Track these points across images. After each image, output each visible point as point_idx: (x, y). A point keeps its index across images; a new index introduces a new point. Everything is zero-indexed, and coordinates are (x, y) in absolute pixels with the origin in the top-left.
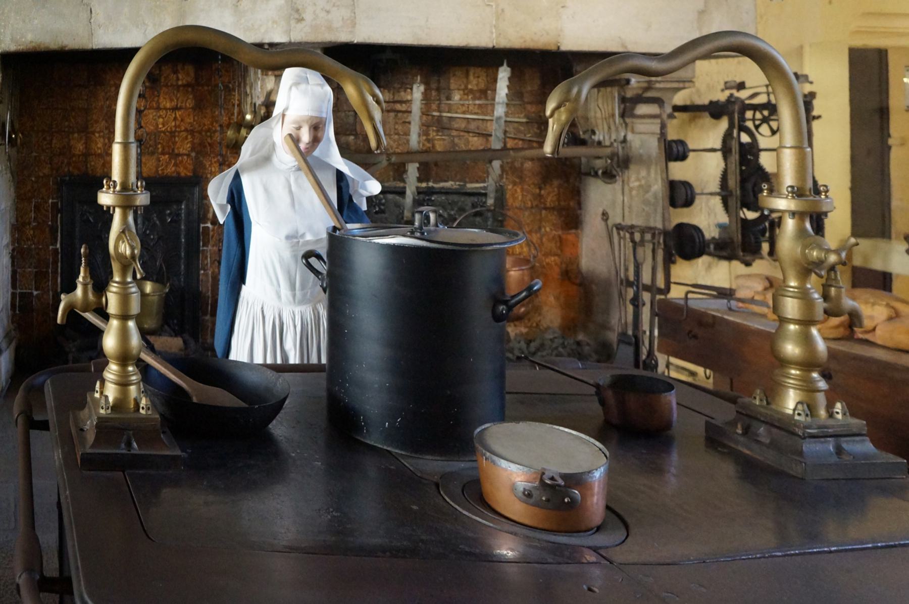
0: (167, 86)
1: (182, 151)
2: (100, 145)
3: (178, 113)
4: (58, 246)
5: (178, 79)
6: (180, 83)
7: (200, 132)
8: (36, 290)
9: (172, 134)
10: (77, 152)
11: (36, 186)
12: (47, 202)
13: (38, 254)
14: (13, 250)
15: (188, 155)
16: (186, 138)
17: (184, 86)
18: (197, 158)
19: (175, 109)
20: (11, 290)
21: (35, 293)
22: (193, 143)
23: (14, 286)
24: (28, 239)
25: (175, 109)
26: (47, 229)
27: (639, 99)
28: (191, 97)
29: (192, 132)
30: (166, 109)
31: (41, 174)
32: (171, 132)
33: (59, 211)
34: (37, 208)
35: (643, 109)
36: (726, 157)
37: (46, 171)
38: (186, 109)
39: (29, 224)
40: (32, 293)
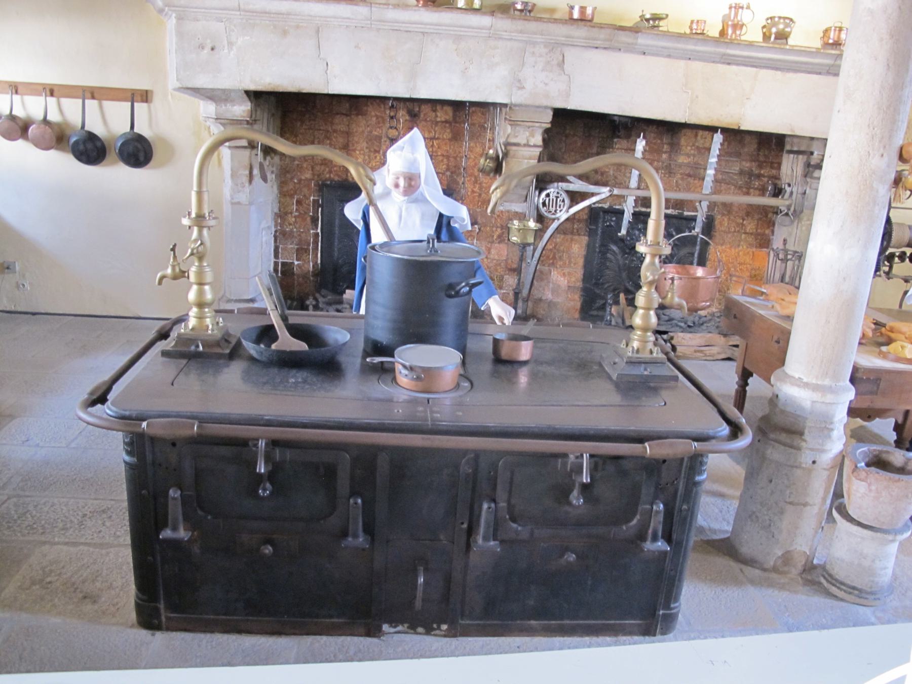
0: (426, 120)
4: (319, 231)
5: (437, 116)
6: (439, 119)
8: (297, 260)
11: (297, 186)
12: (308, 199)
14: (276, 232)
16: (442, 161)
17: (443, 122)
18: (451, 176)
20: (273, 260)
21: (296, 263)
22: (448, 165)
23: (276, 255)
24: (290, 224)
26: (309, 219)
28: (448, 131)
29: (448, 157)
31: (303, 178)
33: (319, 206)
34: (299, 202)
37: (308, 175)
38: (444, 139)
39: (291, 213)
40: (293, 263)
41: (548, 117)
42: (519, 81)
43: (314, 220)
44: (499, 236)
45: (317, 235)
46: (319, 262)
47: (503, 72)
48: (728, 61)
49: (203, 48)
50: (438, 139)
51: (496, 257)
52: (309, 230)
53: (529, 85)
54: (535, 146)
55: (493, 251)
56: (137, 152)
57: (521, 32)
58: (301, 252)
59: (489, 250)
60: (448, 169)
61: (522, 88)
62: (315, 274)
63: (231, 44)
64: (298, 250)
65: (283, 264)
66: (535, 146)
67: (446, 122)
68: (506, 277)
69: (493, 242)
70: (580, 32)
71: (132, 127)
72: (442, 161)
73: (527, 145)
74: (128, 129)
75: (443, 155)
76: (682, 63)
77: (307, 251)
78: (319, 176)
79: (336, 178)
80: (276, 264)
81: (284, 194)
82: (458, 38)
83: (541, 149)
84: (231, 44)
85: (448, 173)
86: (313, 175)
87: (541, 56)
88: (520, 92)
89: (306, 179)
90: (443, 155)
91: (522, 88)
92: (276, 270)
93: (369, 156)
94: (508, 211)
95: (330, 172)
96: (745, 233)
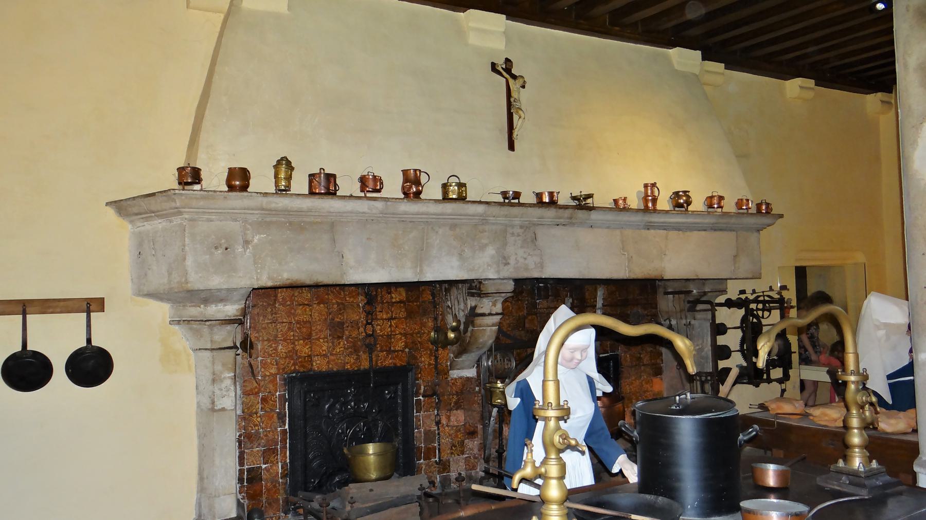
1: (397, 348)
2: (324, 348)
3: (393, 322)
4: (287, 427)
5: (392, 298)
6: (394, 300)
7: (412, 335)
9: (389, 337)
10: (303, 355)
13: (266, 436)
14: (240, 436)
15: (403, 351)
19: (390, 319)
21: (264, 466)
22: (406, 342)
23: (241, 463)
25: (390, 319)
27: (698, 301)
29: (405, 335)
30: (383, 319)
32: (388, 336)
35: (700, 307)
36: (743, 331)
37: (273, 371)
39: (256, 413)
41: (510, 286)
42: (504, 258)
43: (281, 417)
44: (456, 403)
45: (284, 431)
46: (288, 461)
47: (491, 251)
48: (649, 227)
49: (216, 248)
50: (395, 318)
51: (456, 424)
52: (276, 429)
53: (512, 261)
54: (497, 314)
55: (452, 418)
56: (91, 367)
57: (506, 216)
58: (269, 453)
59: (448, 418)
60: (406, 347)
61: (507, 264)
62: (284, 476)
63: (247, 243)
64: (264, 452)
65: (249, 470)
66: (497, 314)
67: (401, 302)
68: (466, 441)
69: (451, 410)
70: (550, 213)
71: (89, 341)
72: (401, 339)
73: (490, 314)
74: (84, 344)
75: (400, 333)
76: (618, 232)
77: (274, 451)
78: (284, 369)
79: (302, 370)
80: (241, 472)
81: (246, 393)
82: (453, 227)
83: (499, 317)
84: (247, 243)
85: (407, 350)
86: (278, 369)
87: (519, 235)
88: (506, 268)
89: (271, 374)
90: (400, 333)
91: (507, 264)
92: (240, 480)
93: (333, 343)
94: (461, 378)
95: (294, 364)
96: (644, 365)
